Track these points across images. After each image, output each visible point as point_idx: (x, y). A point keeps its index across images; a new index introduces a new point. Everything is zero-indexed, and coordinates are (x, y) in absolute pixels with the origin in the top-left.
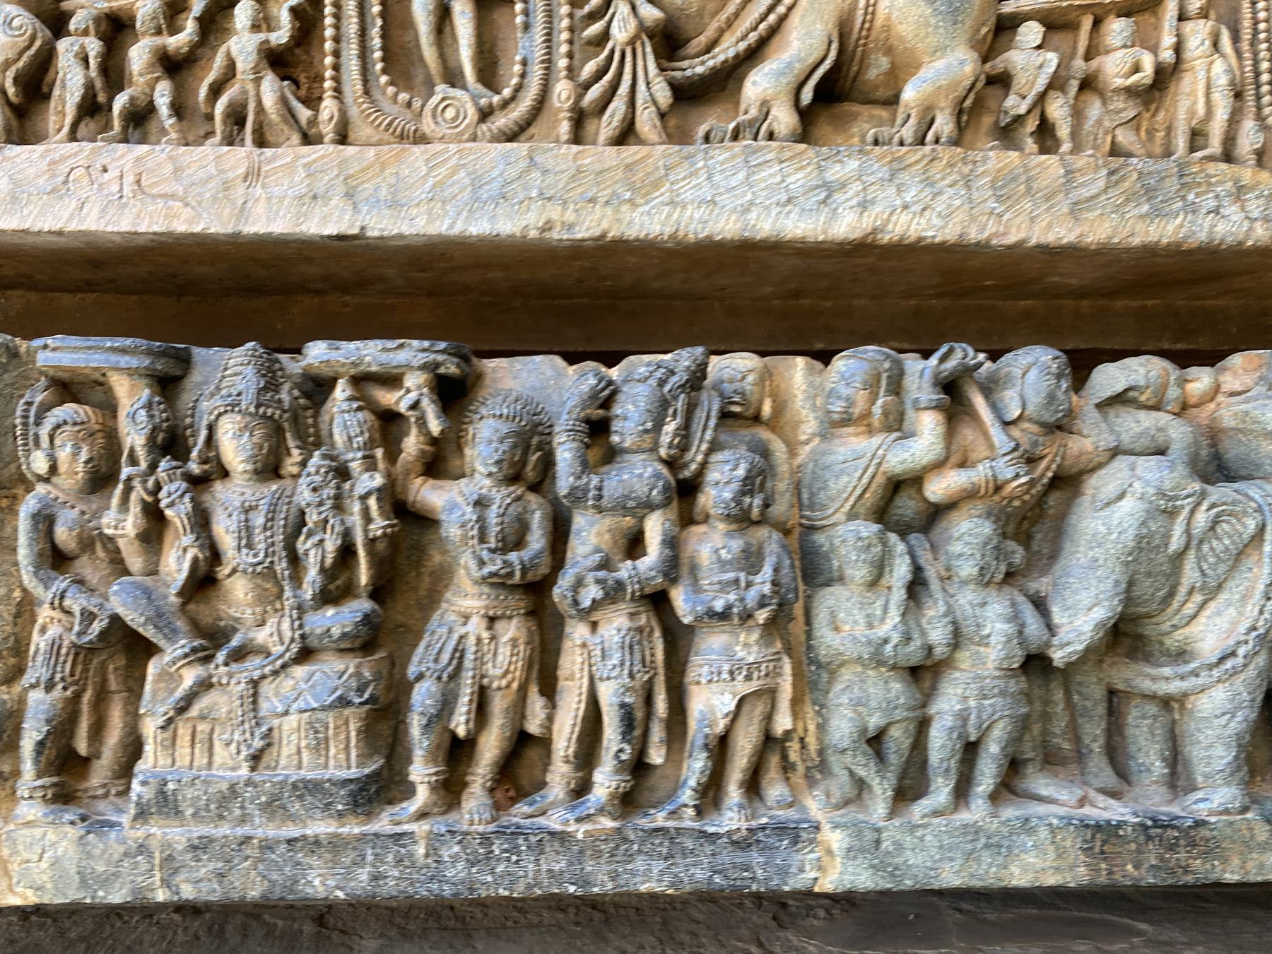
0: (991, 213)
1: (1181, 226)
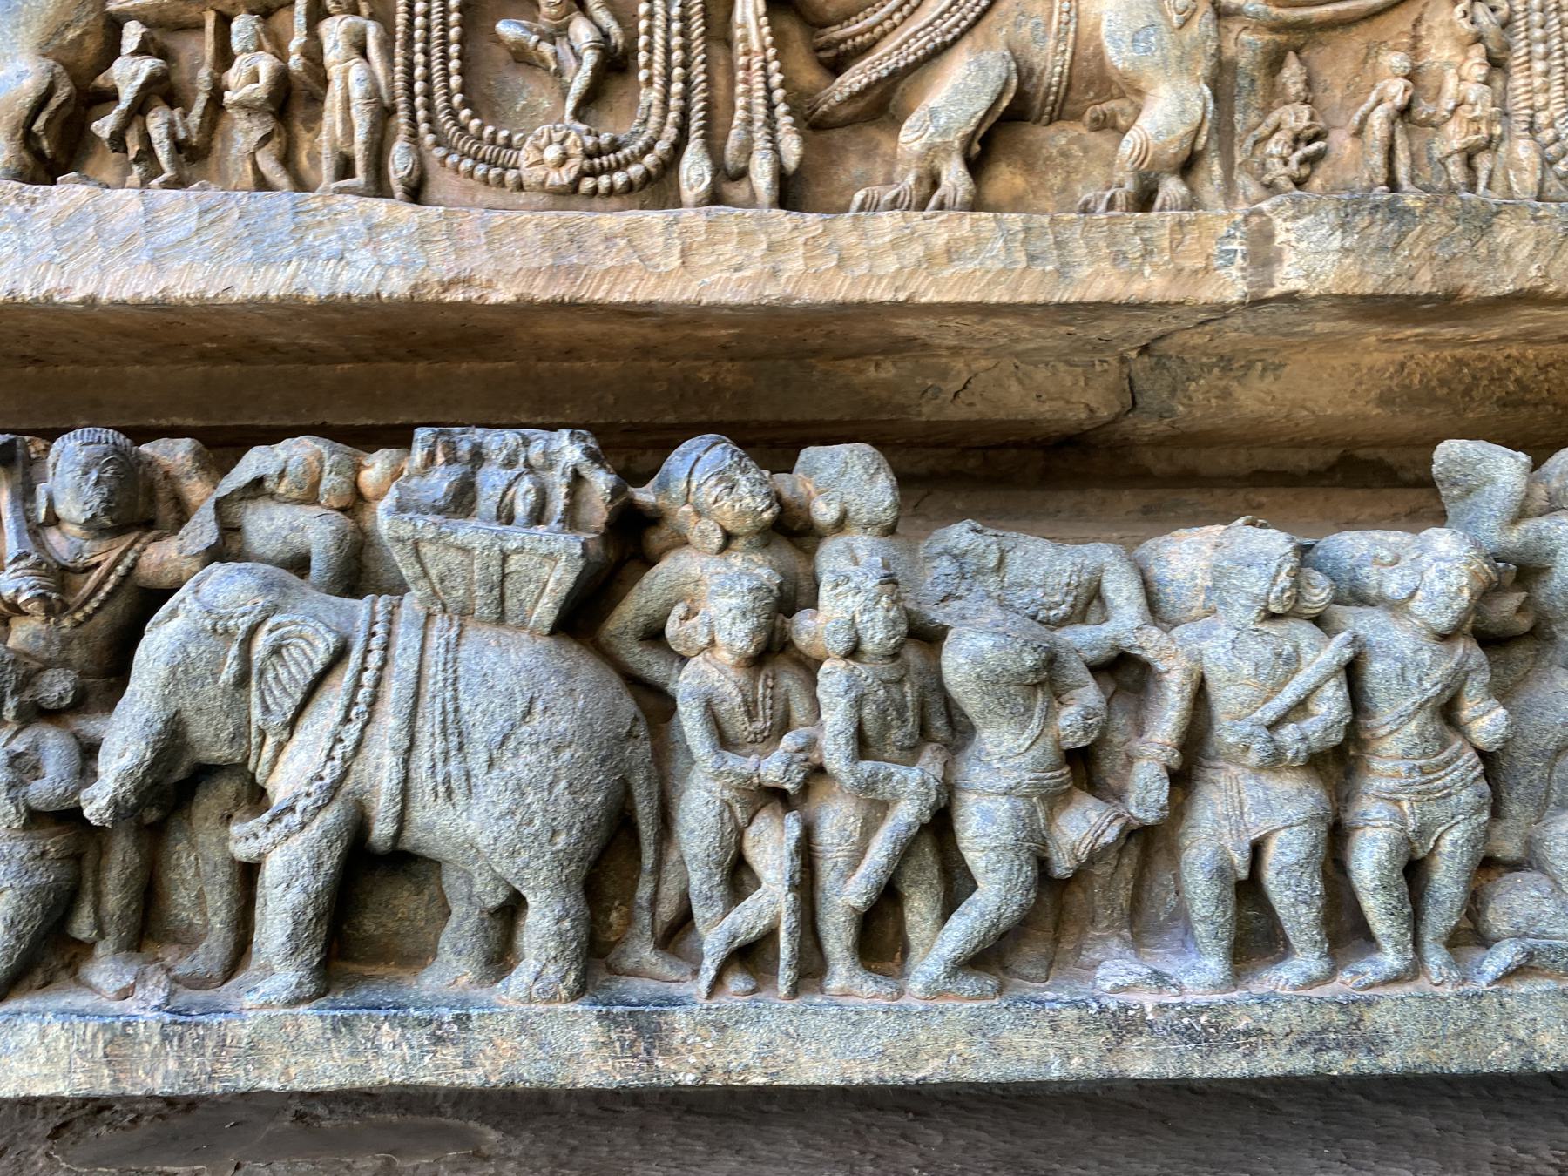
0: (50, 262)
1: (295, 276)
